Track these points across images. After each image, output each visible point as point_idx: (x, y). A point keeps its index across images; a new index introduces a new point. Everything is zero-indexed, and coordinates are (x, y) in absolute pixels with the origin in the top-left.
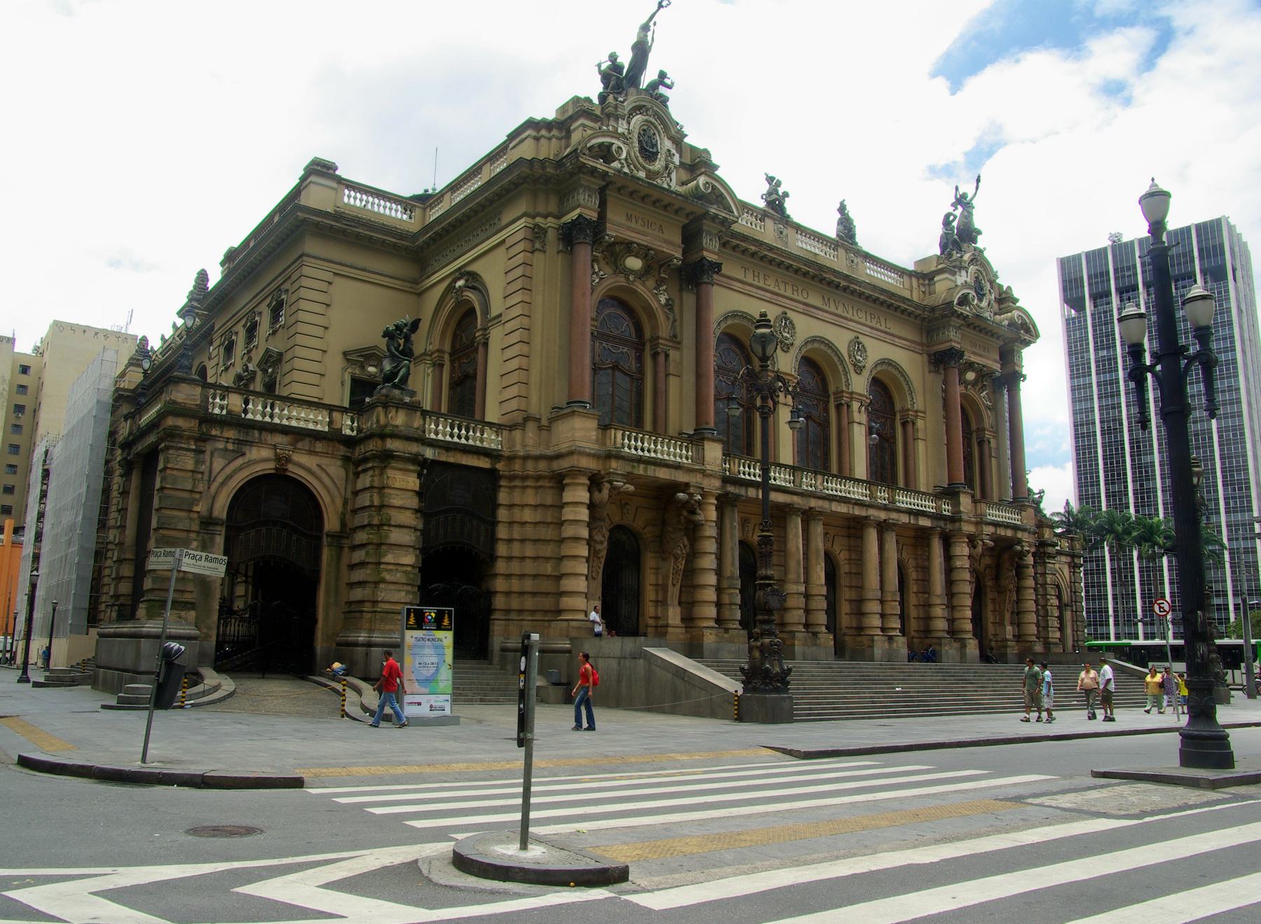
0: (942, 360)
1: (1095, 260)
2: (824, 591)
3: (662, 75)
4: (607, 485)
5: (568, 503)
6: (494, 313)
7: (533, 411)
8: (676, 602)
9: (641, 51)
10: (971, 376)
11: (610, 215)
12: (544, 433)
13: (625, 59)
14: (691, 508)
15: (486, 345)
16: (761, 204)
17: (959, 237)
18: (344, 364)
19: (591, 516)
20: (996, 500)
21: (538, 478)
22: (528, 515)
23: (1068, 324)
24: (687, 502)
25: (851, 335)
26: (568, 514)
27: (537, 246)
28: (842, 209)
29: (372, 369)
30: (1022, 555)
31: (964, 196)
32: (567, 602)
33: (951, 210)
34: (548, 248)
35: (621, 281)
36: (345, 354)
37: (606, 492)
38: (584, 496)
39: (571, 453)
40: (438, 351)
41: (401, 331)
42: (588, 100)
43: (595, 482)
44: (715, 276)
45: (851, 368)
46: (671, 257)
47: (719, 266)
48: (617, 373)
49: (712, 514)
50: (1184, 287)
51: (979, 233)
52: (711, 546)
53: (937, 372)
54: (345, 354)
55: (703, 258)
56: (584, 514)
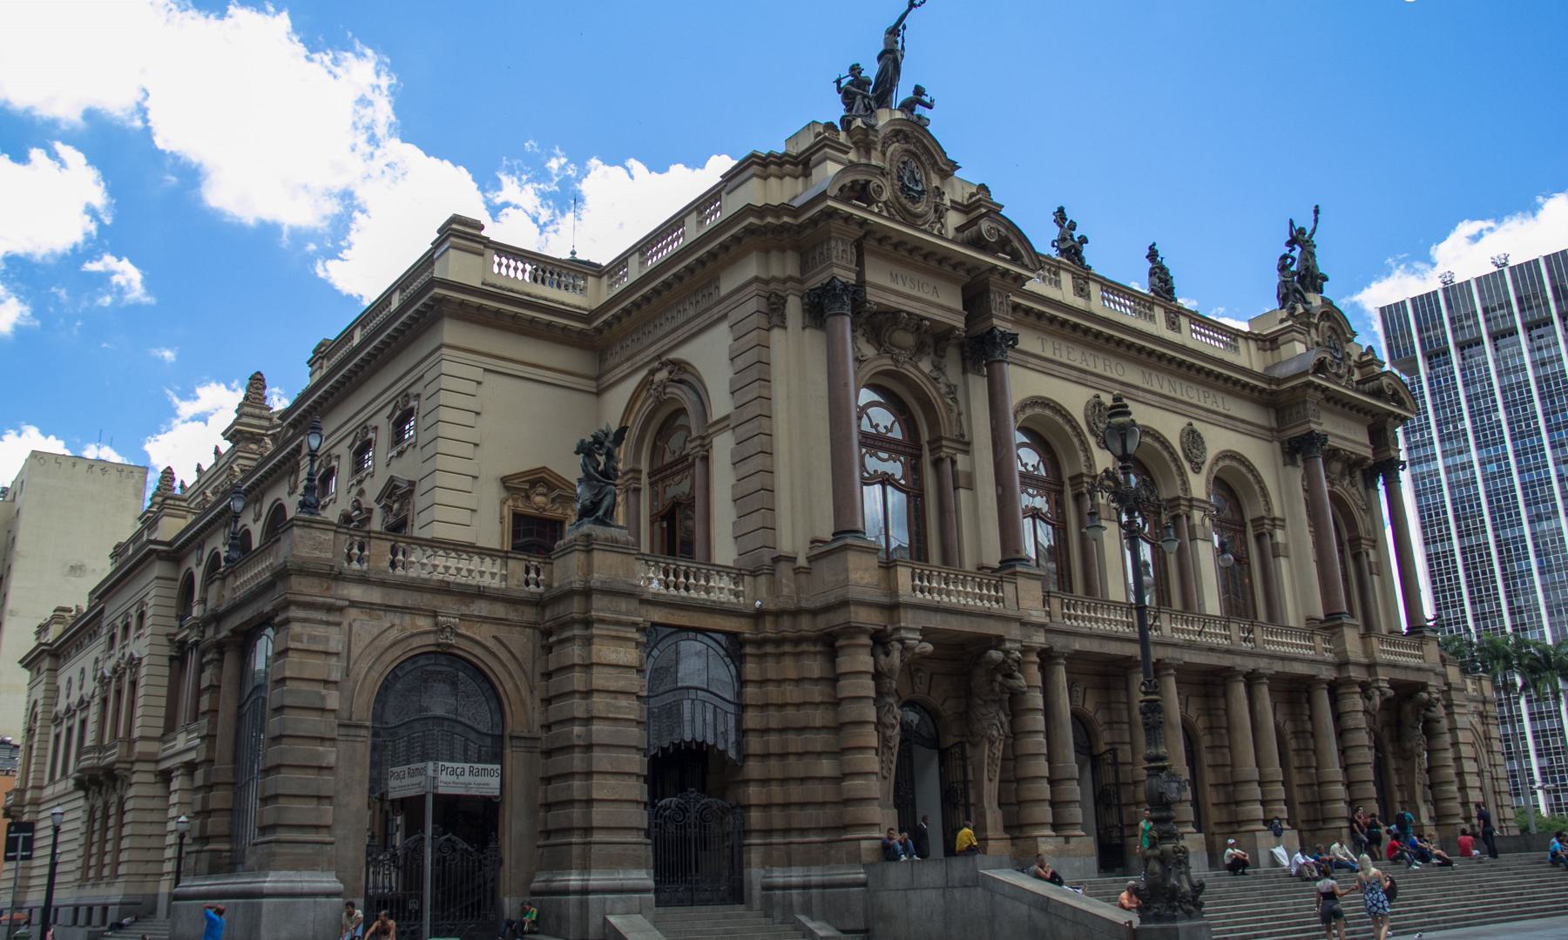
0: (1300, 449)
1: (1423, 306)
2: (1185, 774)
3: (919, 91)
4: (898, 646)
5: (845, 674)
7: (786, 545)
8: (995, 804)
9: (891, 59)
10: (1337, 467)
11: (870, 276)
12: (803, 577)
13: (871, 71)
14: (1006, 670)
15: (706, 459)
16: (1054, 253)
17: (1300, 278)
18: (504, 494)
19: (878, 691)
20: (1384, 632)
21: (797, 641)
22: (791, 693)
24: (1004, 662)
26: (847, 688)
27: (775, 320)
28: (1153, 255)
29: (538, 499)
30: (1429, 705)
31: (1302, 231)
32: (851, 813)
35: (886, 363)
37: (896, 658)
38: (865, 661)
39: (845, 604)
40: (633, 470)
41: (602, 444)
42: (830, 126)
43: (880, 641)
44: (1009, 353)
45: (1187, 466)
46: (954, 328)
47: (1014, 337)
48: (889, 489)
49: (1037, 678)
50: (1540, 337)
51: (1325, 279)
52: (1039, 722)
53: (1294, 463)
55: (993, 328)
56: (868, 687)
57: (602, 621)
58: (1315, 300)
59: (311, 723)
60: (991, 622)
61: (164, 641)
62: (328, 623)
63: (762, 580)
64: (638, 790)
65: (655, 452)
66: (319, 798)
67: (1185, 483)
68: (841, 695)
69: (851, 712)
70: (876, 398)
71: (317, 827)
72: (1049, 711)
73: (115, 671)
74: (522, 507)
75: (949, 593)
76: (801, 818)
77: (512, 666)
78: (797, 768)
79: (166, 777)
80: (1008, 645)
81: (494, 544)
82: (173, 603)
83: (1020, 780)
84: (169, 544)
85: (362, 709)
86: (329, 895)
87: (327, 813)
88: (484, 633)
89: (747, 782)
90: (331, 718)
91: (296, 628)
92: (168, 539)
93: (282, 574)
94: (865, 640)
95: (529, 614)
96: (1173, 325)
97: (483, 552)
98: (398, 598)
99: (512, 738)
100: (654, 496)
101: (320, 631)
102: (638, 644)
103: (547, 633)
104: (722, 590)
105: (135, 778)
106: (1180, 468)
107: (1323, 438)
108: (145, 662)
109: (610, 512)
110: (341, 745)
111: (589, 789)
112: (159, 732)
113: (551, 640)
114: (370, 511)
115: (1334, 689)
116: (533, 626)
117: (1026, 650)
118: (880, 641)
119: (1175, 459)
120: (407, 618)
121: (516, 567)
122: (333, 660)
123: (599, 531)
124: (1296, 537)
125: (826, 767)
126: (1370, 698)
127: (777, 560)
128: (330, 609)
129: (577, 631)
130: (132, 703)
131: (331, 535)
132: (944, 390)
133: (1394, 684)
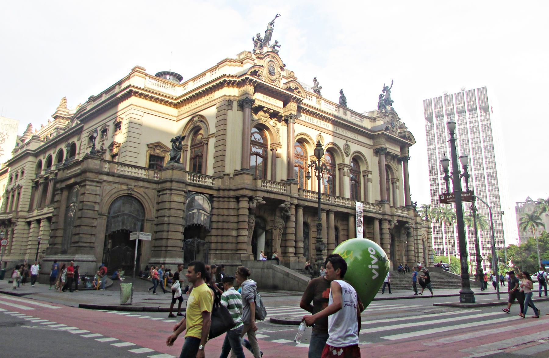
4: (256, 201)
6: (211, 133)
10: (389, 157)
15: (207, 144)
18: (148, 149)
19: (250, 213)
21: (229, 198)
22: (226, 212)
23: (426, 128)
25: (344, 142)
28: (341, 92)
29: (158, 151)
31: (387, 87)
33: (382, 93)
34: (233, 108)
36: (148, 145)
43: (251, 199)
45: (345, 155)
52: (293, 224)
54: (148, 145)
56: (247, 212)
57: (175, 190)
58: (388, 108)
59: (90, 214)
60: (282, 196)
61: (31, 181)
62: (97, 186)
63: (220, 180)
64: (182, 237)
65: (193, 140)
66: (91, 235)
67: (343, 159)
68: (240, 213)
69: (241, 219)
70: (257, 130)
71: (90, 243)
72: (296, 222)
73: (12, 189)
74: (152, 153)
75: (271, 187)
76: (226, 246)
77: (148, 200)
78: (225, 232)
79: (29, 223)
80: (286, 203)
81: (144, 166)
82: (34, 169)
83: (286, 240)
84: (34, 151)
85: (105, 210)
86: (92, 261)
87: (93, 239)
88: (141, 191)
89: (211, 236)
90: (96, 212)
91: (88, 187)
92: (34, 149)
93: (84, 172)
94: (247, 199)
95: (154, 186)
96: (345, 114)
97: (142, 168)
98: (117, 180)
99: (147, 220)
100: (191, 153)
101: (95, 188)
102: (184, 196)
103: (159, 191)
104: (208, 182)
105: (18, 223)
106: (342, 155)
107: (386, 149)
108: (23, 187)
109: (179, 159)
110: (99, 220)
111: (168, 235)
112: (27, 209)
113: (160, 193)
114: (106, 150)
115: (381, 221)
116: (155, 189)
117: (292, 204)
118: (251, 199)
119: (341, 153)
120: (119, 186)
121: (151, 172)
122: (98, 196)
123: (176, 164)
124: (375, 176)
125: (234, 233)
126: (391, 225)
127: (225, 175)
128: (98, 182)
129: (168, 192)
130: (18, 199)
131: (99, 162)
132: (276, 130)
133: (398, 221)
